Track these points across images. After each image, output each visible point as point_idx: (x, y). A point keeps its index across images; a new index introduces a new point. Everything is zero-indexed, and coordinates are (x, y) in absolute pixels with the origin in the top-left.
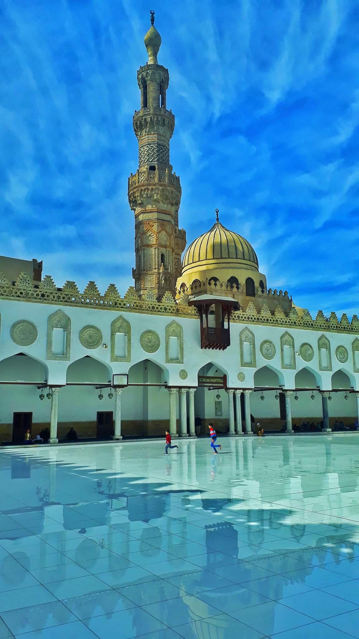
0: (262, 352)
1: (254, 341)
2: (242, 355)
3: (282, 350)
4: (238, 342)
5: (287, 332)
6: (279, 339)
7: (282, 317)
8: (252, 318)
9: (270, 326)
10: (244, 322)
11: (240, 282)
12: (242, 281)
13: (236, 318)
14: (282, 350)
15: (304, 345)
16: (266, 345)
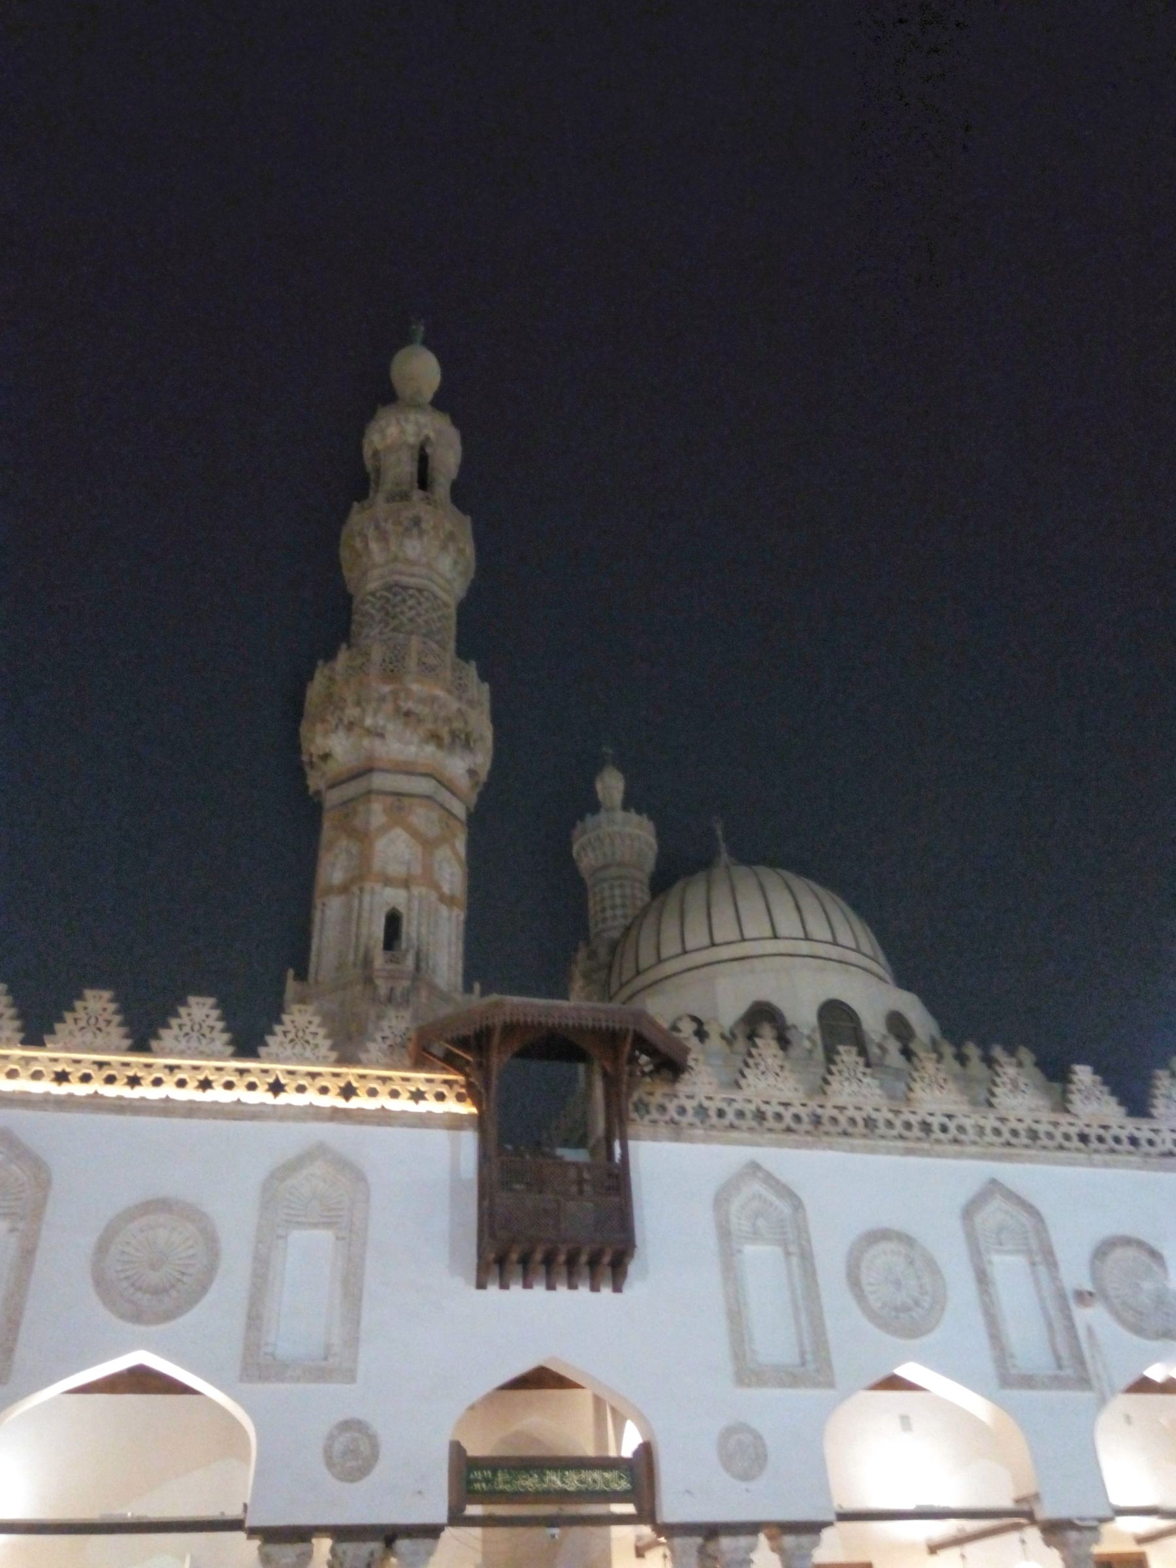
0: (859, 1294)
1: (802, 1231)
2: (736, 1315)
3: (983, 1278)
4: (711, 1242)
5: (994, 1187)
6: (955, 1224)
7: (950, 1108)
8: (779, 1117)
9: (889, 1151)
10: (734, 1134)
11: (790, 1017)
12: (803, 1016)
13: (690, 1117)
14: (983, 1278)
15: (1104, 1250)
16: (882, 1257)
